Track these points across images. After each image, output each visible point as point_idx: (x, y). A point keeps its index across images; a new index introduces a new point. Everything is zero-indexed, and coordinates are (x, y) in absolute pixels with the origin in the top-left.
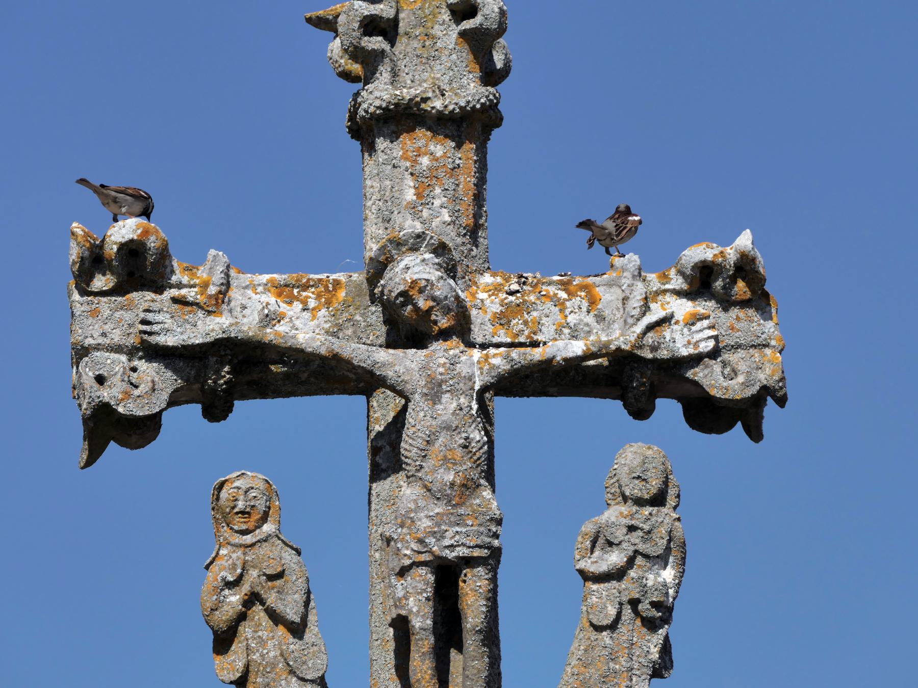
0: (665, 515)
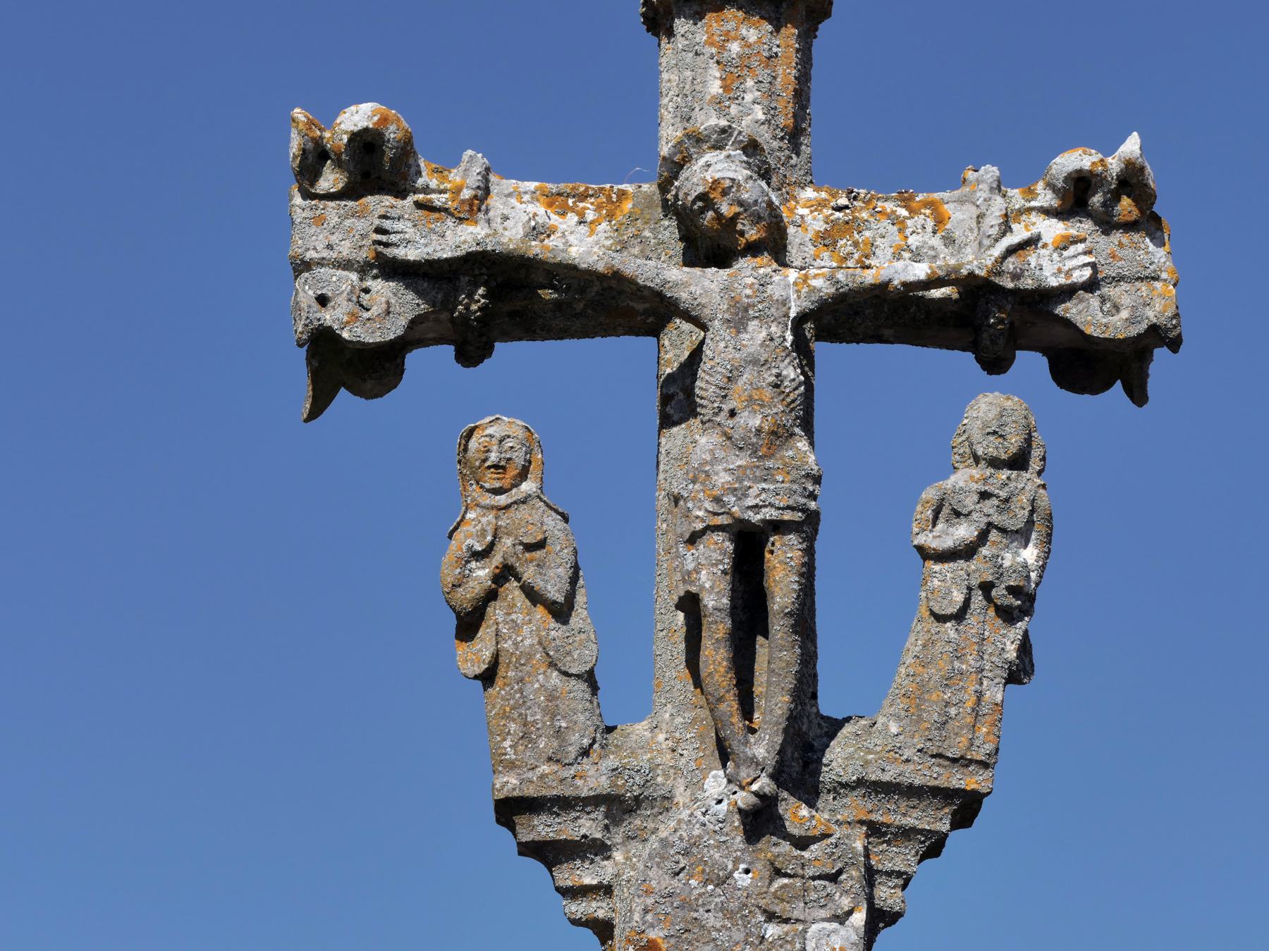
0: (1026, 483)
